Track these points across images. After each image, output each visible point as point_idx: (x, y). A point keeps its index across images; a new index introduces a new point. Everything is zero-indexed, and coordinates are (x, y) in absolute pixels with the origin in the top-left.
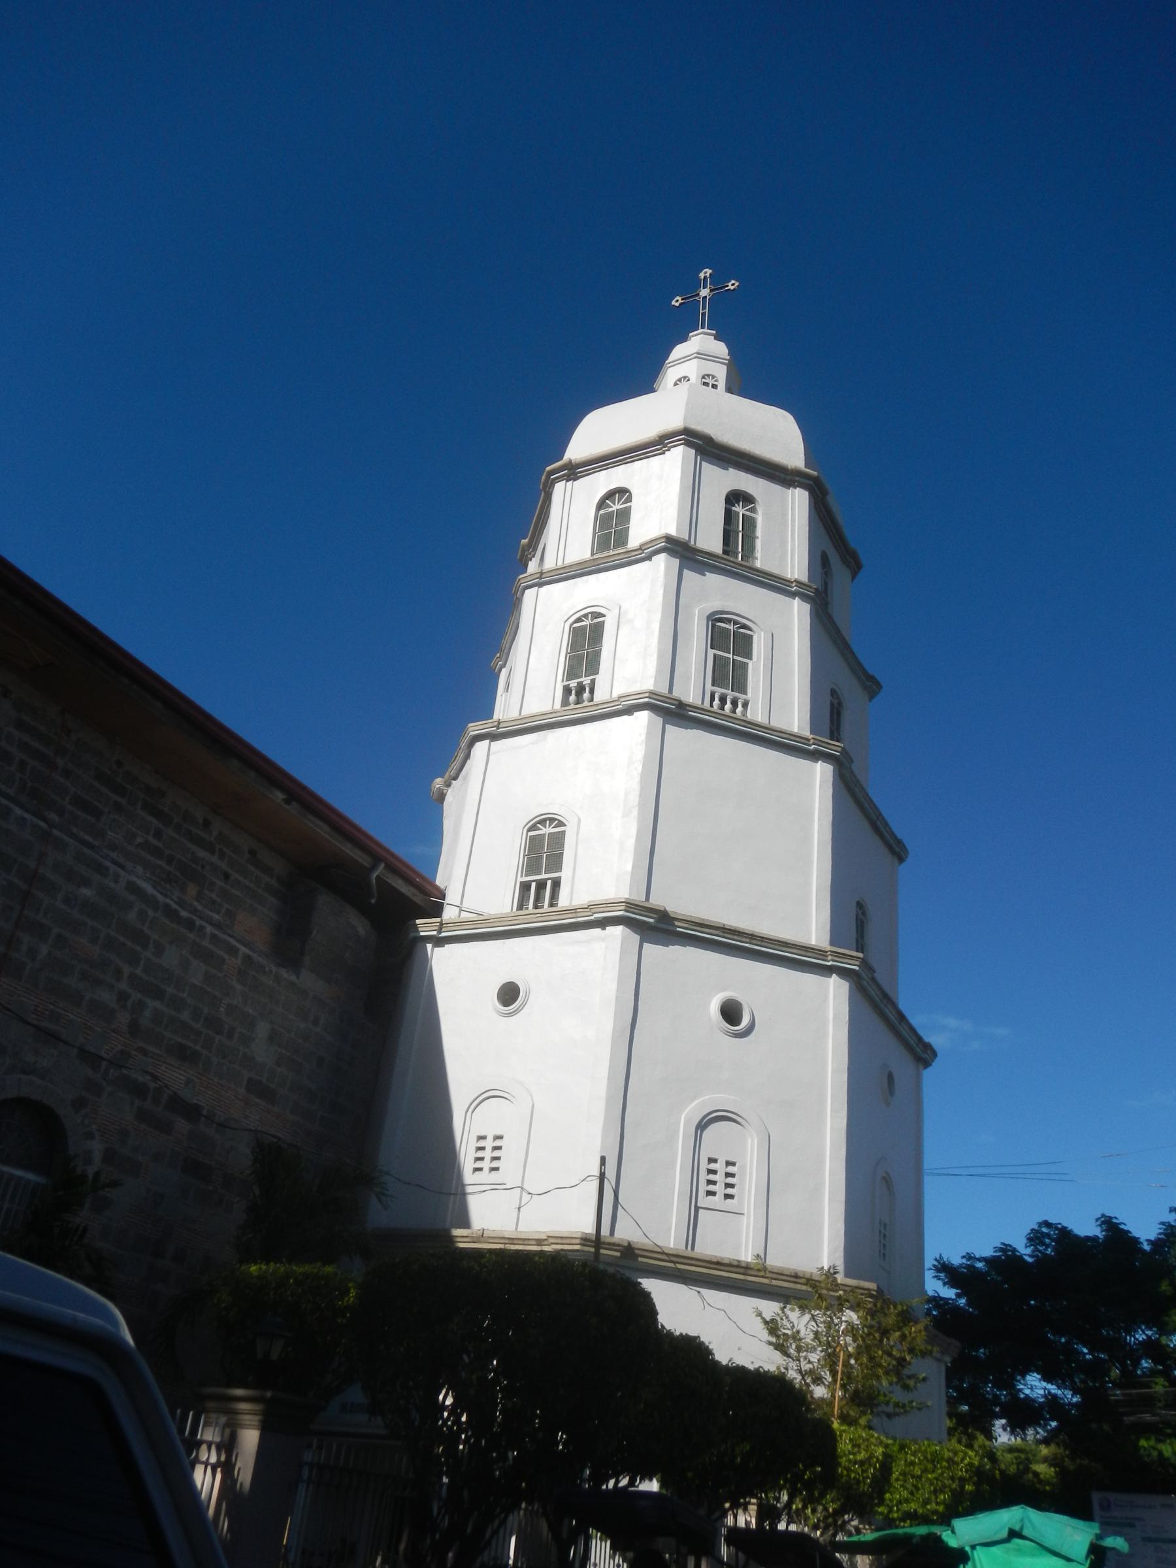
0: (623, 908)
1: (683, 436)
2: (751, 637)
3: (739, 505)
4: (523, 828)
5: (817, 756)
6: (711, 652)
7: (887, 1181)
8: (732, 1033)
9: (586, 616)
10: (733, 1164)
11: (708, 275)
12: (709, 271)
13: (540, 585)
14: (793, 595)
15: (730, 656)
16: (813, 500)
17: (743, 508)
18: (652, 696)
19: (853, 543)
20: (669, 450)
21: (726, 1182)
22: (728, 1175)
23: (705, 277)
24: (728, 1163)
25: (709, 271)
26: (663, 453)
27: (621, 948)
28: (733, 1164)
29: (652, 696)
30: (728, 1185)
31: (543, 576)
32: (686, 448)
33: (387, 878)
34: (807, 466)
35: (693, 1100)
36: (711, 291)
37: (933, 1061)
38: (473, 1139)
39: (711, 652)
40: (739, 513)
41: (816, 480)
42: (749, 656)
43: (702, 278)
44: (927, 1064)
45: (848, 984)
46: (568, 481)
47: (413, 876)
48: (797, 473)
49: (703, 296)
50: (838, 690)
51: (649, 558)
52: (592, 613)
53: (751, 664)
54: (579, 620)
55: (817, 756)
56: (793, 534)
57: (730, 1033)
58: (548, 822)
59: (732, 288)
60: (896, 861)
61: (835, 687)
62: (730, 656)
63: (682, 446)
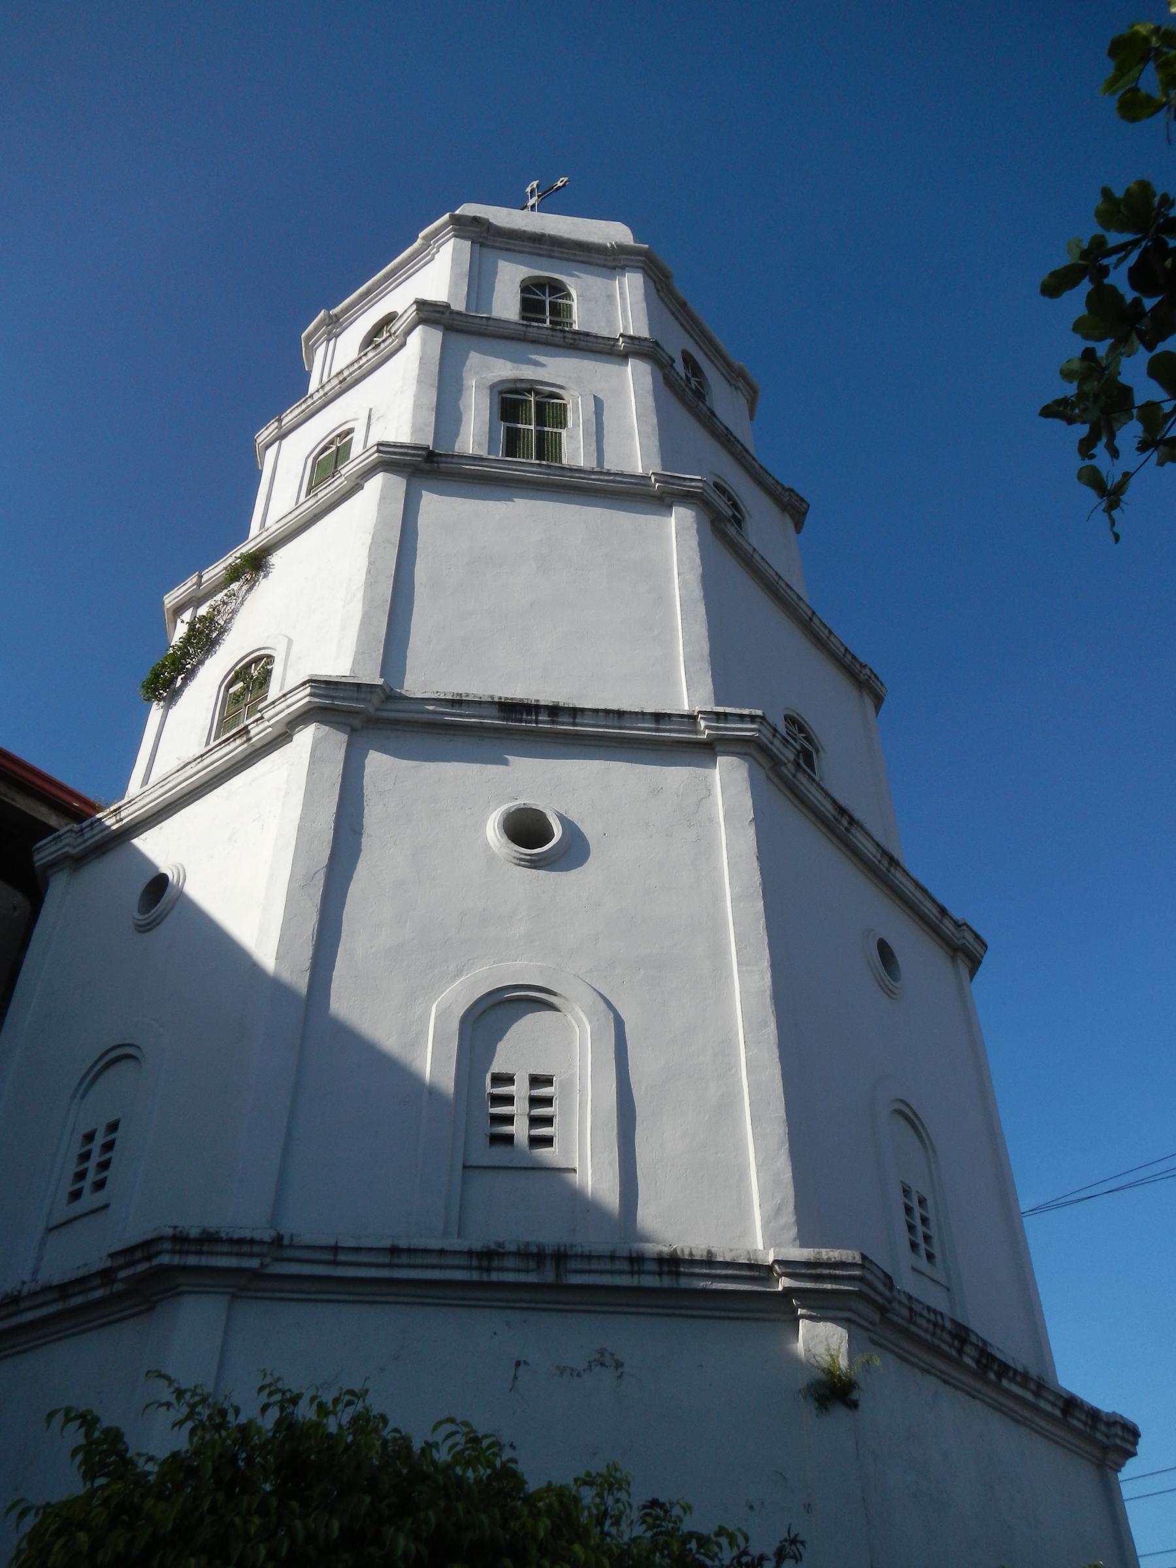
0: (308, 691)
1: (451, 226)
2: (565, 405)
3: (544, 294)
4: (220, 687)
5: (668, 500)
6: (502, 426)
7: (908, 1116)
8: (528, 861)
9: (332, 442)
10: (548, 1081)
11: (535, 186)
12: (535, 183)
13: (282, 437)
14: (624, 357)
15: (532, 427)
16: (652, 284)
17: (550, 296)
18: (382, 448)
19: (738, 363)
20: (438, 251)
21: (532, 1114)
22: (535, 1101)
23: (532, 191)
24: (537, 1081)
25: (535, 183)
26: (432, 259)
27: (312, 756)
28: (548, 1081)
29: (382, 448)
30: (535, 1121)
31: (283, 423)
32: (457, 239)
33: (14, 800)
34: (635, 241)
35: (459, 973)
36: (539, 196)
37: (982, 957)
38: (78, 1138)
39: (502, 426)
40: (544, 302)
41: (647, 254)
42: (562, 423)
43: (529, 191)
44: (974, 963)
45: (746, 764)
46: (329, 340)
47: (67, 798)
48: (621, 250)
49: (531, 204)
50: (722, 483)
51: (403, 345)
52: (338, 436)
53: (564, 433)
54: (325, 449)
55: (668, 500)
56: (624, 311)
57: (521, 859)
58: (253, 665)
59: (561, 184)
60: (869, 703)
61: (719, 481)
62: (532, 427)
63: (452, 240)
